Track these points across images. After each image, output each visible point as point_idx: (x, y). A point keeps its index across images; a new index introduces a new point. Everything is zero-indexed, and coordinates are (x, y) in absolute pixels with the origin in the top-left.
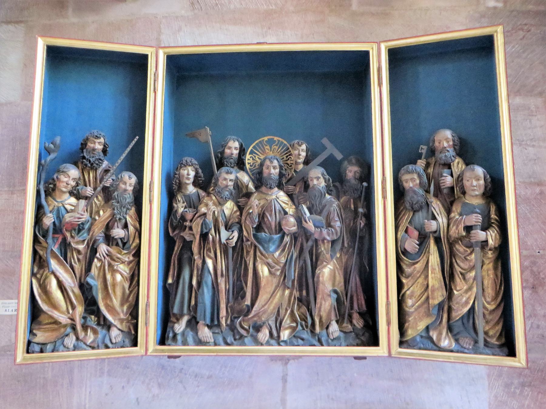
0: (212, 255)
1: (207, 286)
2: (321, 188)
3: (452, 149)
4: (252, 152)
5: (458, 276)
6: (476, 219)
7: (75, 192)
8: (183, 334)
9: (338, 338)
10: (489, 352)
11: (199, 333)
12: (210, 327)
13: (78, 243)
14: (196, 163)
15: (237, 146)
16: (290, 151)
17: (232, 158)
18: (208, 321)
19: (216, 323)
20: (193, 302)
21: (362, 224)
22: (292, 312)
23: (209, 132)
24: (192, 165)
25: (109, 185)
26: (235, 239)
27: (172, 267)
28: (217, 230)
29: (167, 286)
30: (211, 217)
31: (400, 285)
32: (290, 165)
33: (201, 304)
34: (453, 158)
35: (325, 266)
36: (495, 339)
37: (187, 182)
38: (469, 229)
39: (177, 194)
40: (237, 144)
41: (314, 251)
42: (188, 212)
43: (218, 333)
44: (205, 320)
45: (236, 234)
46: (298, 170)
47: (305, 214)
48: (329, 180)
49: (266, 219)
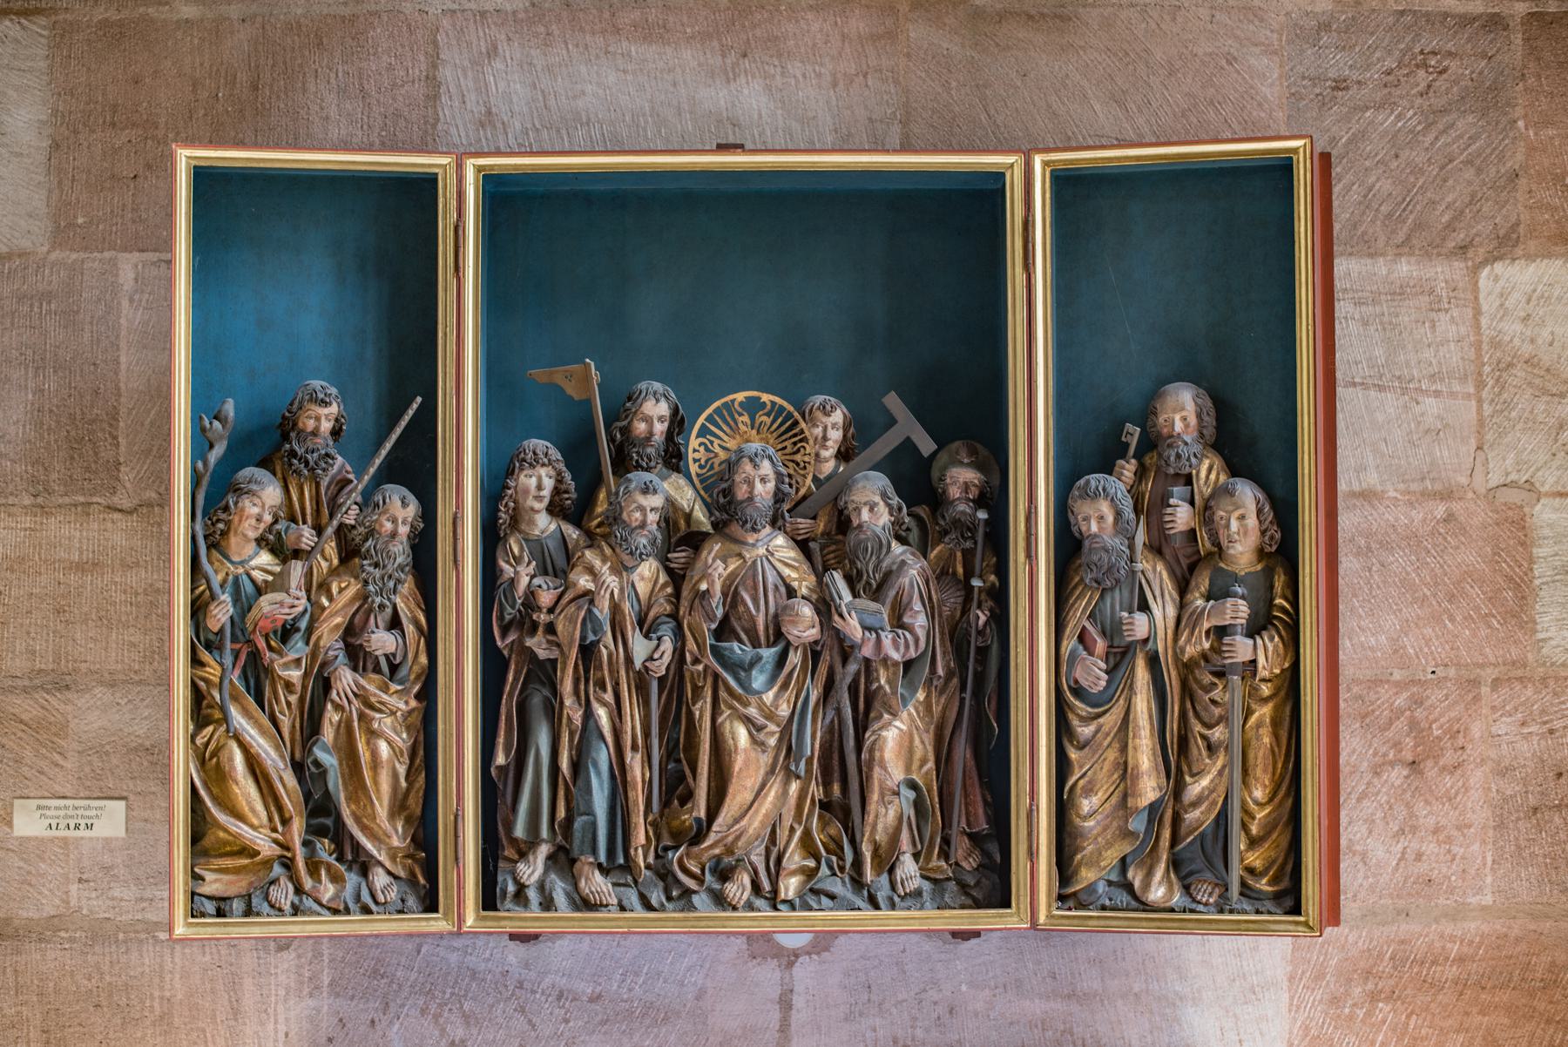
0: (609, 697)
1: (599, 774)
2: (878, 530)
4: (704, 432)
6: (1238, 610)
7: (271, 537)
8: (541, 887)
9: (918, 893)
10: (1248, 908)
11: (582, 883)
12: (605, 871)
13: (286, 666)
14: (560, 458)
16: (802, 432)
18: (602, 858)
19: (621, 861)
20: (561, 813)
21: (983, 618)
22: (807, 834)
24: (550, 464)
25: (353, 522)
26: (667, 658)
29: (493, 772)
30: (607, 604)
31: (1062, 767)
32: (802, 464)
33: (585, 818)
34: (1193, 460)
37: (537, 506)
38: (1221, 632)
40: (663, 409)
41: (862, 687)
42: (545, 587)
43: (626, 885)
44: (594, 851)
45: (668, 646)
46: (822, 477)
47: (840, 598)
48: (900, 509)
49: (741, 609)
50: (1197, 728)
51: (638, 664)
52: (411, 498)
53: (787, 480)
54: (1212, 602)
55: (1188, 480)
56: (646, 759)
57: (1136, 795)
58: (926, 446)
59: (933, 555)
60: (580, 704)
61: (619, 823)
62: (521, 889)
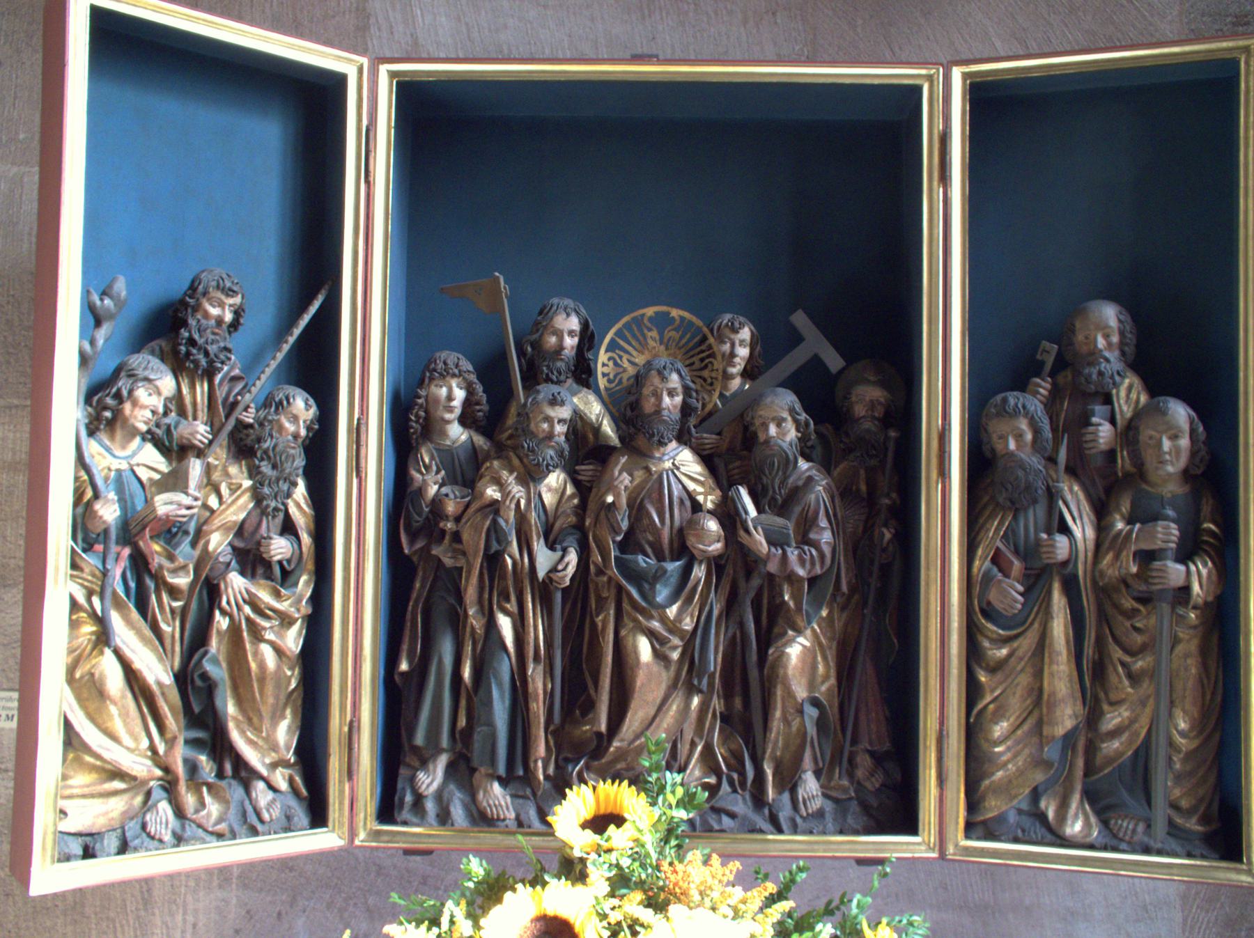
0: (512, 606)
1: (500, 685)
2: (785, 446)
3: (1117, 353)
4: (612, 347)
5: (1116, 670)
6: (1168, 533)
8: (439, 796)
9: (820, 814)
10: (1179, 849)
11: (481, 795)
12: (504, 782)
14: (471, 368)
15: (574, 328)
16: (710, 347)
17: (562, 359)
18: (502, 770)
19: (521, 773)
20: (462, 722)
21: (888, 536)
22: (708, 749)
23: (505, 288)
24: (460, 375)
26: (571, 570)
27: (407, 633)
28: (525, 543)
29: (397, 678)
30: (512, 514)
31: (973, 691)
32: (709, 380)
33: (484, 728)
34: (1117, 378)
35: (792, 641)
36: (1194, 820)
37: (448, 416)
38: (1147, 557)
39: (418, 444)
40: (574, 323)
41: (765, 601)
42: (452, 496)
43: (524, 797)
44: (493, 762)
45: (572, 558)
46: (728, 394)
47: (746, 512)
48: (807, 424)
49: (646, 522)
50: (1117, 653)
51: (541, 574)
52: (311, 402)
53: (694, 394)
54: (1138, 526)
55: (1107, 400)
56: (548, 669)
57: (1053, 723)
58: (834, 361)
59: (836, 473)
60: (483, 614)
61: (519, 734)
62: (419, 799)
